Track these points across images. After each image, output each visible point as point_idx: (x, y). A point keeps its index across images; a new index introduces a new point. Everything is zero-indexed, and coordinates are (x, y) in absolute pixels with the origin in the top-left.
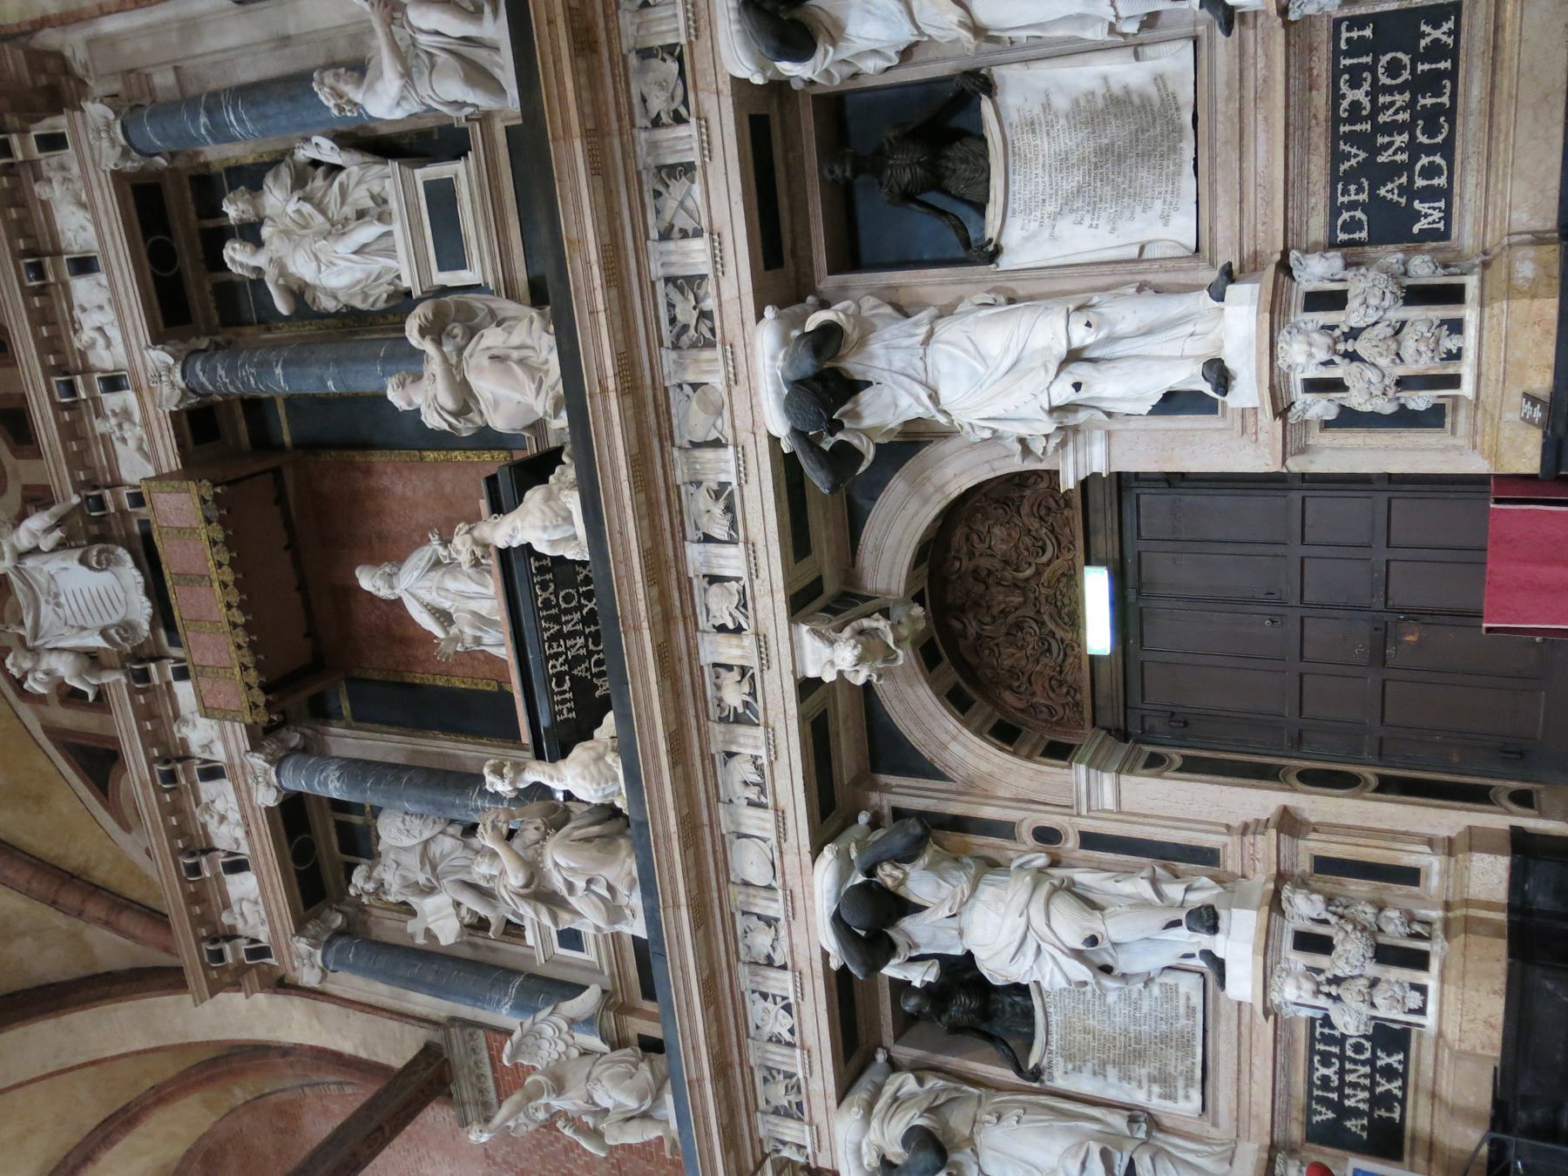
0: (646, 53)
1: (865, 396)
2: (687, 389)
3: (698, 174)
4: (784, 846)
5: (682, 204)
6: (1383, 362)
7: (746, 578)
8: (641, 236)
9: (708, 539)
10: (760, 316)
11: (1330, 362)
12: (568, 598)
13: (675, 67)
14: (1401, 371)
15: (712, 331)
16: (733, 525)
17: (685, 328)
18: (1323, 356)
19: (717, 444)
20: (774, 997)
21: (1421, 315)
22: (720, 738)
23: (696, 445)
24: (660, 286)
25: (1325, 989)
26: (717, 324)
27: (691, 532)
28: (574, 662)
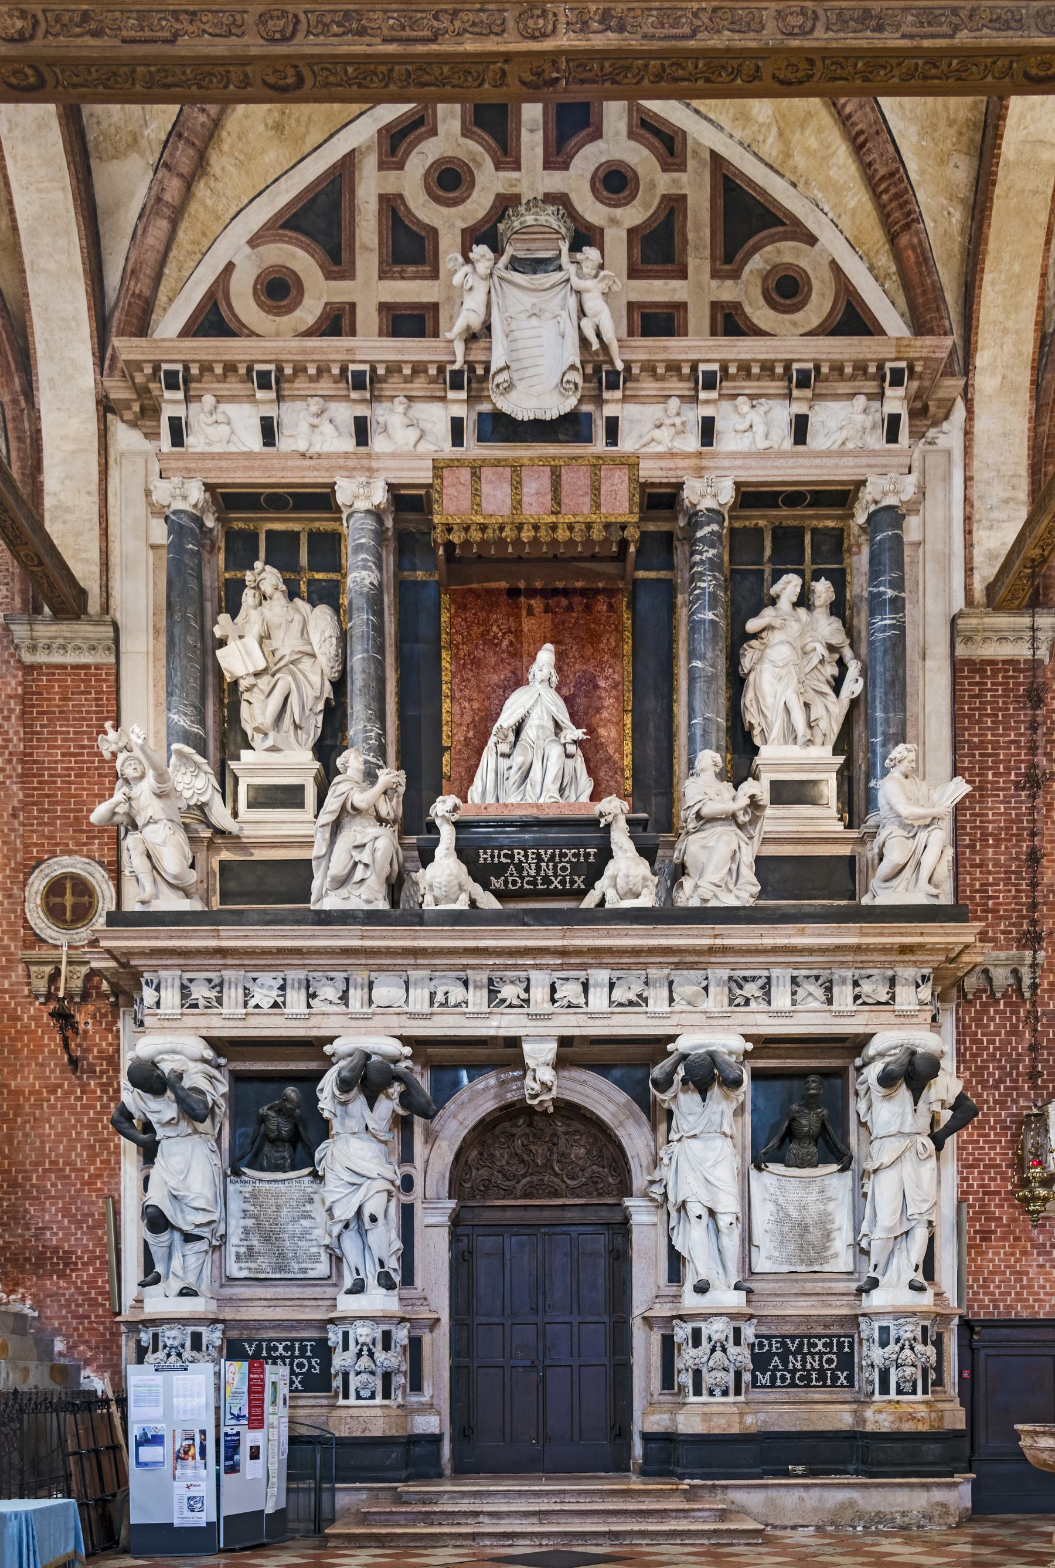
0: (892, 982)
1: (697, 1097)
2: (704, 983)
3: (825, 1007)
4: (404, 1017)
5: (810, 994)
6: (711, 1363)
7: (589, 1010)
8: (796, 966)
9: (612, 986)
10: (747, 1037)
11: (710, 1339)
12: (564, 869)
13: (883, 1000)
14: (705, 1370)
15: (738, 1005)
16: (620, 1005)
17: (741, 987)
18: (715, 1337)
19: (671, 1000)
20: (284, 996)
21: (730, 1378)
22: (478, 978)
23: (671, 983)
24: (765, 973)
25: (365, 1348)
26: (743, 1009)
27: (618, 974)
28: (519, 868)
